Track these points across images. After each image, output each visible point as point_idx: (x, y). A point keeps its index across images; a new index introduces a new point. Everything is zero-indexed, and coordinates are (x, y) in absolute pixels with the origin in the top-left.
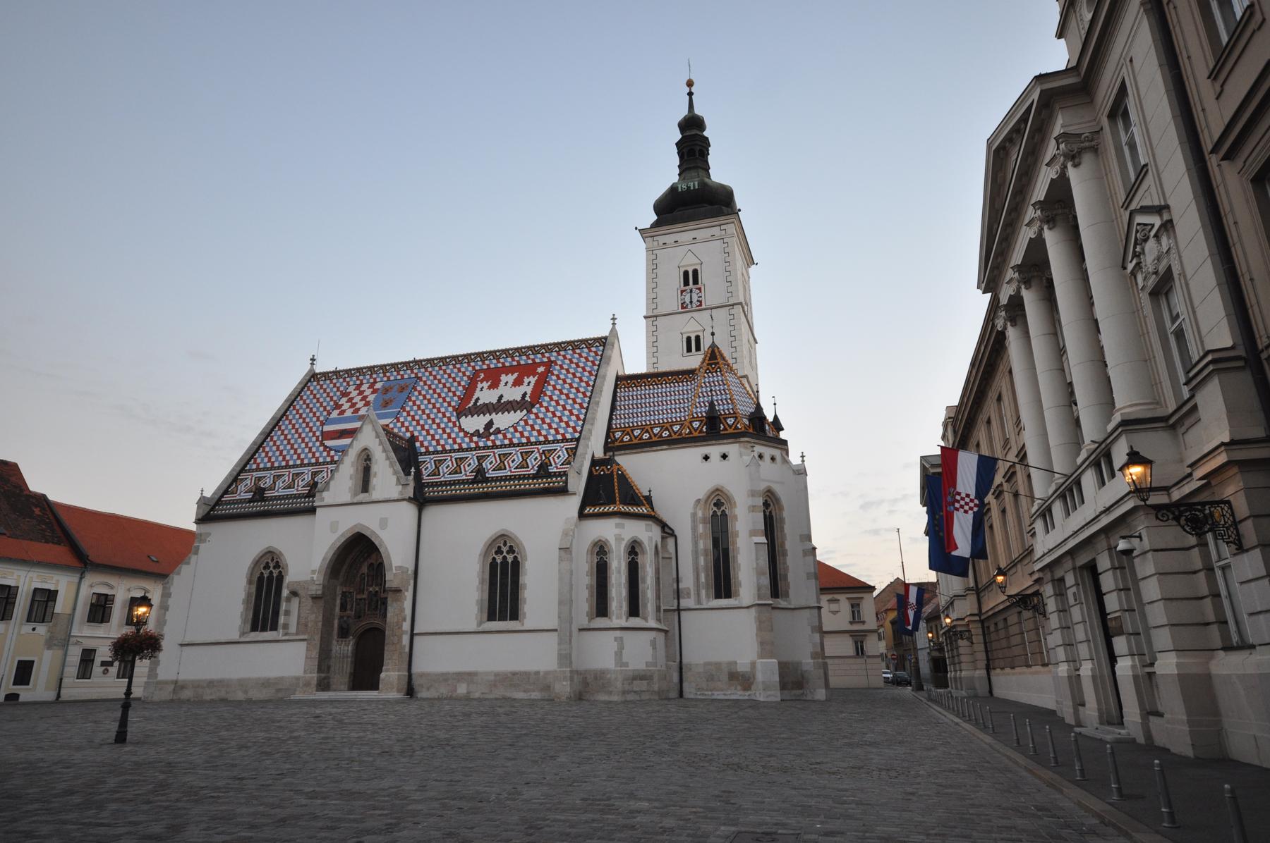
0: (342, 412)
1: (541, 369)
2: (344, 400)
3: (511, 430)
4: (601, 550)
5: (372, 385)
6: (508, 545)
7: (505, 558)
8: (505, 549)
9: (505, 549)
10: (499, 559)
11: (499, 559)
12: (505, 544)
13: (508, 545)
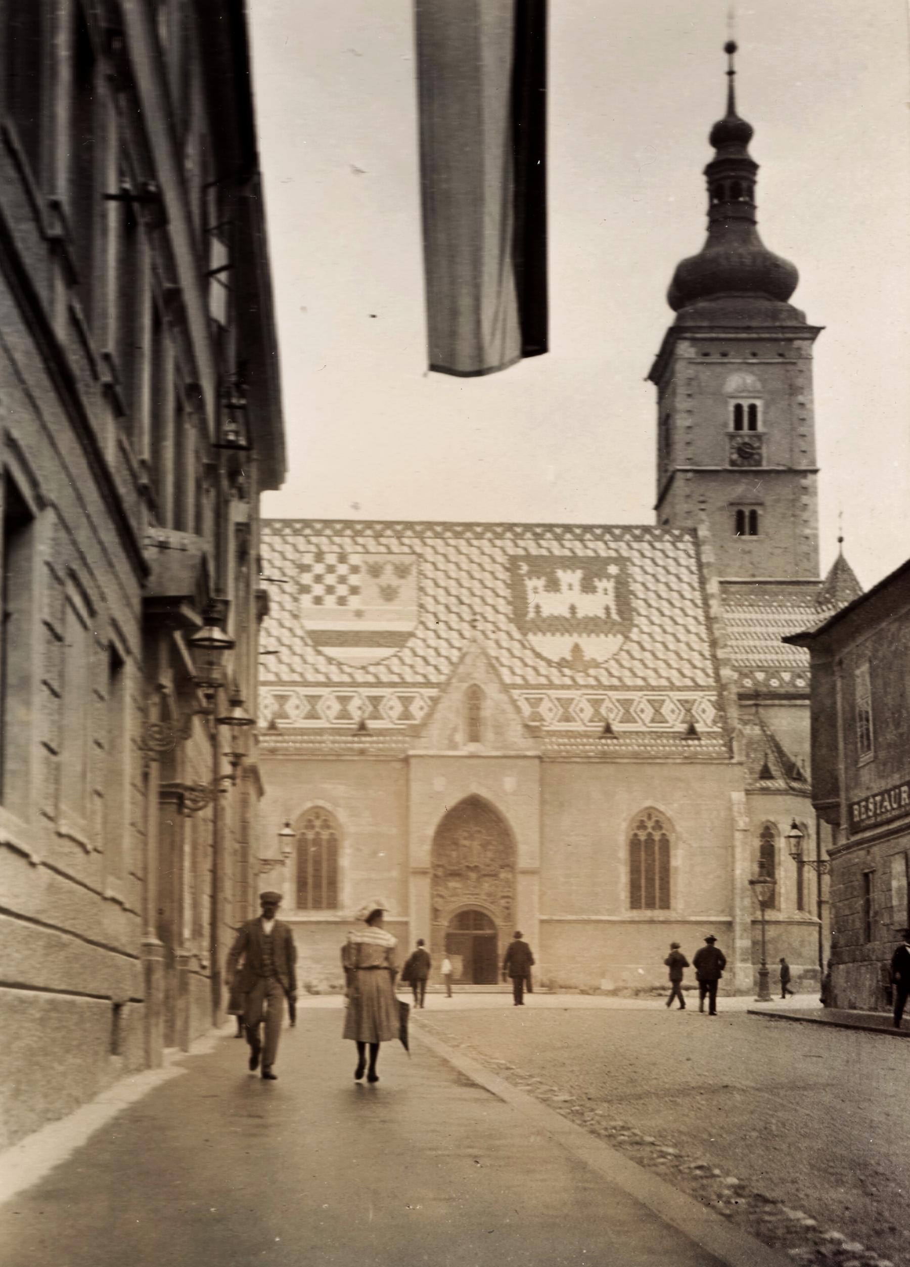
0: (318, 600)
1: (613, 569)
2: (306, 579)
3: (612, 663)
4: (768, 833)
5: (342, 558)
6: (654, 819)
7: (650, 835)
8: (650, 824)
9: (650, 824)
10: (642, 836)
11: (642, 836)
12: (650, 817)
13: (654, 819)
